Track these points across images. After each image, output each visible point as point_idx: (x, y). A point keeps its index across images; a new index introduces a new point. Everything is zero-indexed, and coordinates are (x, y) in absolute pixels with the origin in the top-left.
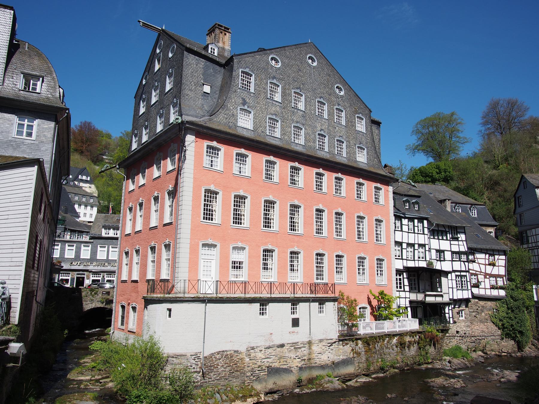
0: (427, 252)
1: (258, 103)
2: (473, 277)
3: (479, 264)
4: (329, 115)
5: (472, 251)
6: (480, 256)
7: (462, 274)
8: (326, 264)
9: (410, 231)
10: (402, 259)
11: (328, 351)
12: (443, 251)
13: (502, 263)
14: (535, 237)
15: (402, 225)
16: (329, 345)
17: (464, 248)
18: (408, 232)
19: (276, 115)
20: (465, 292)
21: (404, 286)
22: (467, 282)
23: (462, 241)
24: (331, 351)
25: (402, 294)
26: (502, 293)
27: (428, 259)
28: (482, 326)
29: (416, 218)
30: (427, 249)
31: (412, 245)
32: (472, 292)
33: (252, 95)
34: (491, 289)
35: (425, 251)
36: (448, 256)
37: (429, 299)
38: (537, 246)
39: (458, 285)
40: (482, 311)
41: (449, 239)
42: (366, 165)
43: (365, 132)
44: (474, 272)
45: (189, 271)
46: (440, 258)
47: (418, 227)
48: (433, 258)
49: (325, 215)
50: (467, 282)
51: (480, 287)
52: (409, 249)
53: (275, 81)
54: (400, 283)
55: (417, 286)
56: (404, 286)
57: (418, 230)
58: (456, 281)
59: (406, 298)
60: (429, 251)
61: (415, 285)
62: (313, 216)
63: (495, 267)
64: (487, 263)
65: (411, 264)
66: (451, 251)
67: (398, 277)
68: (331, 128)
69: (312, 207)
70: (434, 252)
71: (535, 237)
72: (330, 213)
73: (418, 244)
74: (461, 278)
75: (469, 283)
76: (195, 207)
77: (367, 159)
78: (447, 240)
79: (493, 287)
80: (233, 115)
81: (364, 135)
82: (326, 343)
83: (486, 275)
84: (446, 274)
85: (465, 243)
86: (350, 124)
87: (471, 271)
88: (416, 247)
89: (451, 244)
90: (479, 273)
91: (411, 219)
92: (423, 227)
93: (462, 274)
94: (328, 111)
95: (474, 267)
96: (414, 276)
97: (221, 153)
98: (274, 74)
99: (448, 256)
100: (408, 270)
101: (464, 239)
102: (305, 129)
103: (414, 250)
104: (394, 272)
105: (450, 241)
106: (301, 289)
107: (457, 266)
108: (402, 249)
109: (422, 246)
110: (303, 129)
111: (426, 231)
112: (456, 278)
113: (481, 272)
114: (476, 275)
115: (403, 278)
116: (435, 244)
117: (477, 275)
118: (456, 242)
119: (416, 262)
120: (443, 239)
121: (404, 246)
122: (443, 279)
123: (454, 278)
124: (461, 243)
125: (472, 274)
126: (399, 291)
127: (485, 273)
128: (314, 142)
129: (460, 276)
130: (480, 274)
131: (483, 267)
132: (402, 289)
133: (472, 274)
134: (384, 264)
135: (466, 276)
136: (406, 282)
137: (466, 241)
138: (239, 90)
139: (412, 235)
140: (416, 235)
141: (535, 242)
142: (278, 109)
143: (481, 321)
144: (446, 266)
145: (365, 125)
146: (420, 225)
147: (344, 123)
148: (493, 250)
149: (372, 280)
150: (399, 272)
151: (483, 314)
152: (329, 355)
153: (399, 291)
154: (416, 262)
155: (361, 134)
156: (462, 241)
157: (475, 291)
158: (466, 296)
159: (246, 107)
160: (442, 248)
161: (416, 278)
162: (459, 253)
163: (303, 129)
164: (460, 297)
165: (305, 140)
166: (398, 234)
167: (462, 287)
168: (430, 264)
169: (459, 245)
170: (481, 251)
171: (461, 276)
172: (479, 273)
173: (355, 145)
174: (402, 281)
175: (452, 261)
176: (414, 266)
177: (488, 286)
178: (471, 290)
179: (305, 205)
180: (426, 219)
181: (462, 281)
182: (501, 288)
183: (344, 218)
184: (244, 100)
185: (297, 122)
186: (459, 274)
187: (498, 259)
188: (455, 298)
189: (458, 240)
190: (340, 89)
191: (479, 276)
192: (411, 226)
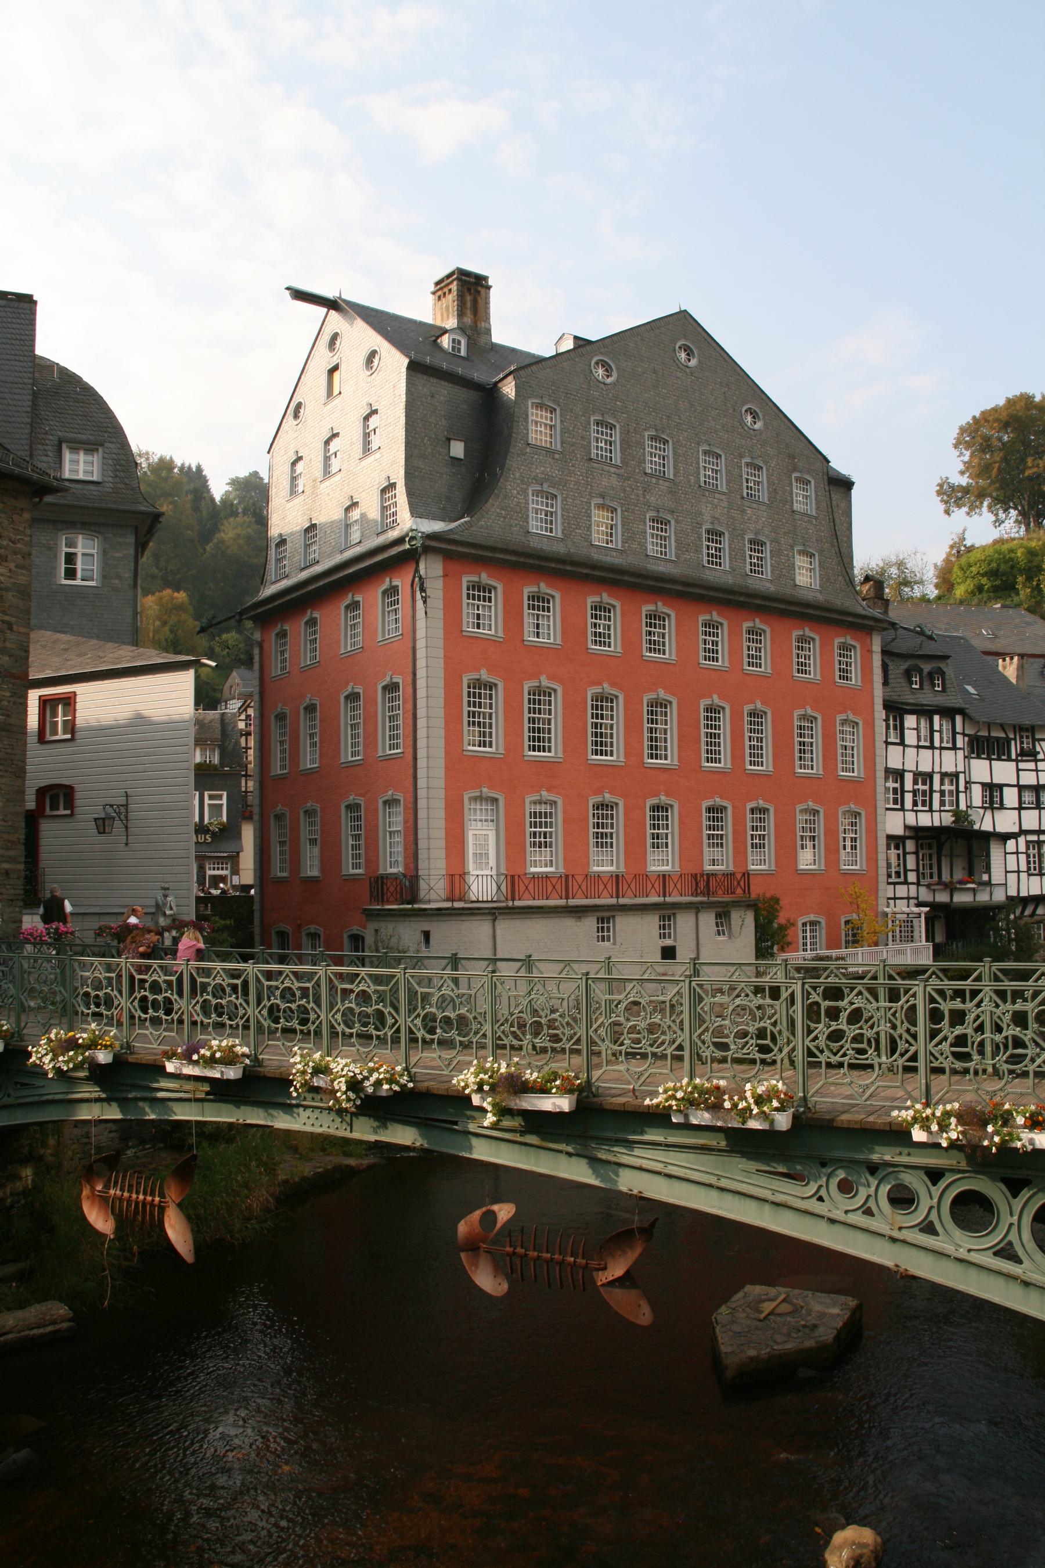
4: (728, 482)
10: (902, 809)
12: (1001, 787)
25: (902, 891)
27: (963, 806)
29: (936, 712)
31: (928, 777)
33: (557, 456)
37: (962, 898)
39: (1032, 865)
41: (1014, 757)
42: (818, 595)
43: (814, 513)
45: (448, 856)
46: (992, 802)
47: (940, 731)
48: (974, 805)
49: (725, 721)
55: (935, 870)
56: (906, 871)
58: (1028, 856)
59: (908, 898)
61: (931, 868)
62: (699, 722)
65: (925, 820)
68: (735, 514)
70: (977, 791)
72: (736, 716)
77: (821, 580)
78: (1009, 759)
81: (811, 523)
84: (1005, 837)
86: (780, 500)
88: (937, 779)
89: (1018, 770)
92: (954, 733)
94: (728, 472)
96: (930, 848)
99: (1011, 797)
100: (917, 833)
102: (677, 521)
104: (882, 842)
105: (1017, 761)
106: (679, 886)
112: (1028, 848)
116: (980, 770)
118: (1031, 765)
119: (936, 815)
120: (999, 759)
121: (909, 778)
122: (996, 853)
123: (1022, 848)
126: (895, 884)
128: (698, 551)
132: (902, 879)
138: (528, 450)
142: (614, 481)
144: (1006, 822)
145: (813, 496)
147: (764, 497)
153: (895, 884)
154: (936, 815)
155: (806, 519)
161: (934, 851)
163: (673, 522)
166: (895, 751)
169: (1037, 770)
173: (792, 547)
174: (901, 862)
175: (1020, 808)
176: (930, 824)
180: (961, 712)
186: (1034, 838)
188: (1024, 893)
189: (1036, 761)
190: (755, 416)
192: (924, 732)
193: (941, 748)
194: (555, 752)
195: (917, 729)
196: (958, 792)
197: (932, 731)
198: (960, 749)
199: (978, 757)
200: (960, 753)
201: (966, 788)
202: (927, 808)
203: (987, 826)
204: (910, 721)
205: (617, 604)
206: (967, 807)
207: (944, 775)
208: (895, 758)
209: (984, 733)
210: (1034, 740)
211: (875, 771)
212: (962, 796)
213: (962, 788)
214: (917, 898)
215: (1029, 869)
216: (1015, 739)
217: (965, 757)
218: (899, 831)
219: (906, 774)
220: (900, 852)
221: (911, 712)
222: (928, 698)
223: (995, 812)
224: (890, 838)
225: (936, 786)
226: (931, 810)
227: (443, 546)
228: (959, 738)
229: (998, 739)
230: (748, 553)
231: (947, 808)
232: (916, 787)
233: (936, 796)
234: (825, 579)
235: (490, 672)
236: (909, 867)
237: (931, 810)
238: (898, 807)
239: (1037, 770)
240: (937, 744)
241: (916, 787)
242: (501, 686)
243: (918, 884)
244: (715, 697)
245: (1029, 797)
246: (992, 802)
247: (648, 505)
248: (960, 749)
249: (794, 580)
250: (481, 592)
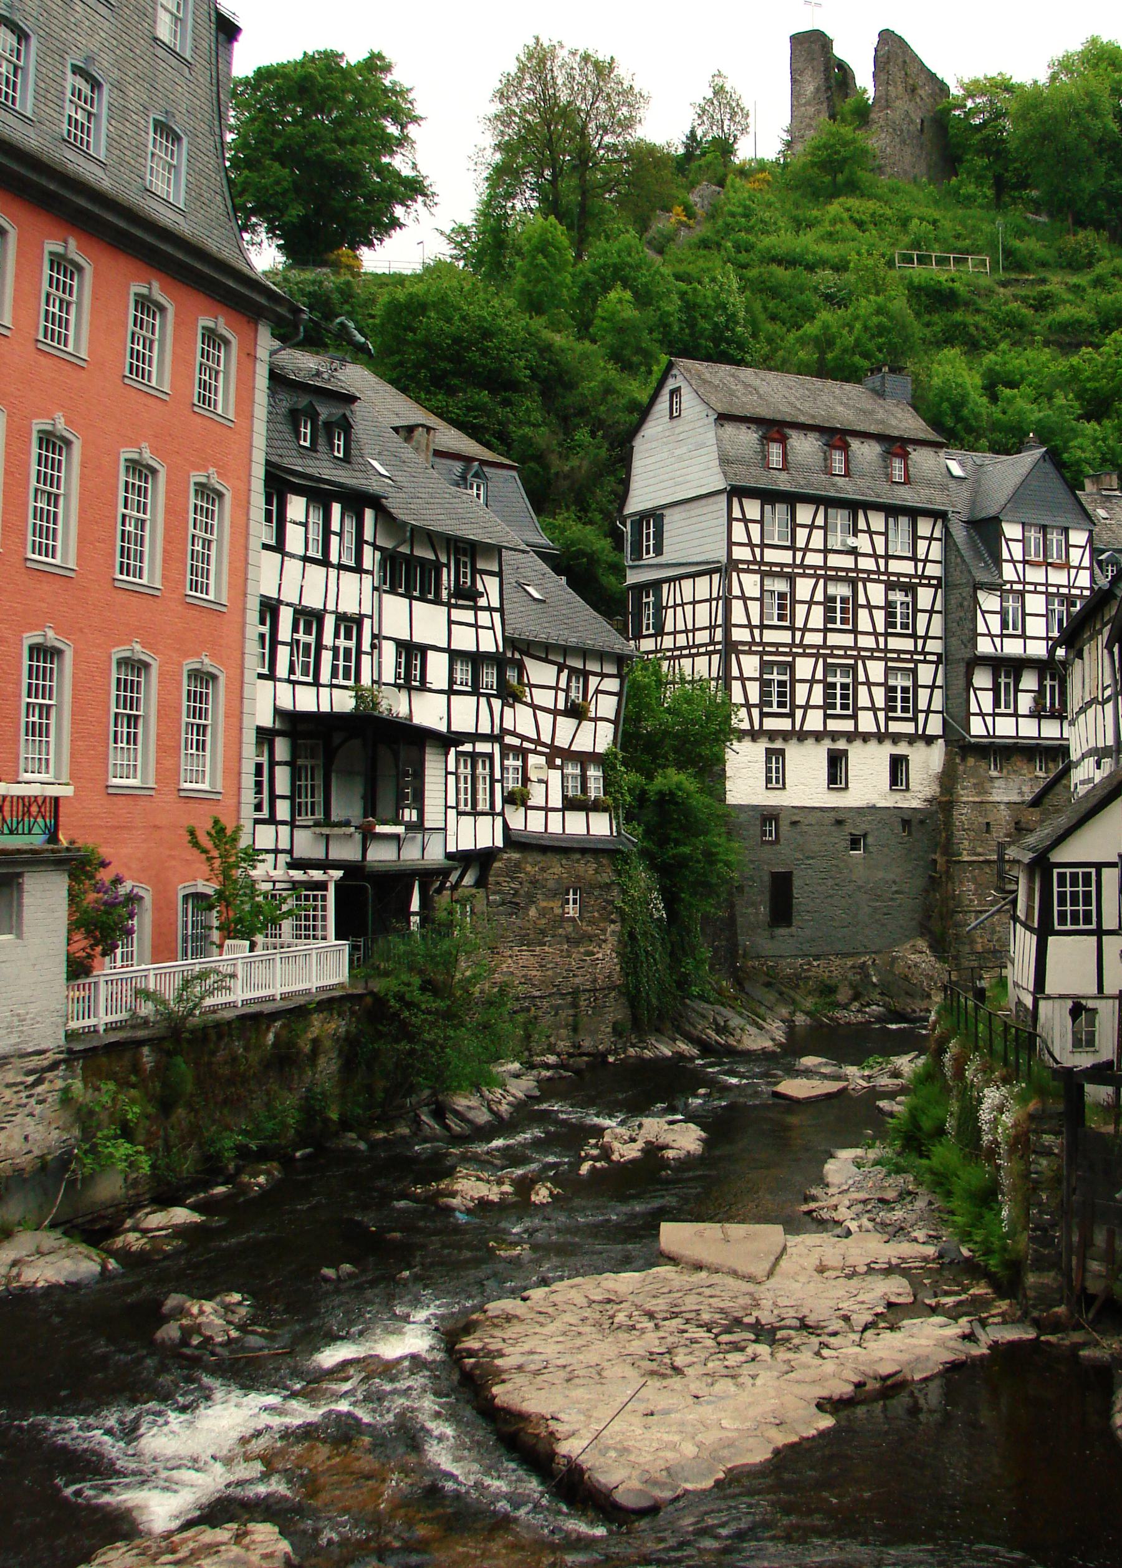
2: (510, 762)
3: (535, 707)
5: (517, 656)
6: (540, 672)
7: (483, 747)
11: (27, 1110)
12: (423, 649)
13: (607, 706)
14: (689, 609)
16: (31, 1079)
17: (488, 644)
20: (485, 822)
21: (273, 797)
23: (490, 609)
24: (38, 1109)
26: (601, 825)
27: (366, 680)
28: (526, 957)
32: (505, 825)
34: (563, 810)
38: (694, 646)
40: (531, 900)
44: (516, 742)
46: (408, 677)
47: (340, 534)
50: (493, 781)
51: (530, 803)
55: (319, 799)
56: (273, 797)
59: (276, 851)
63: (585, 723)
64: (561, 706)
65: (307, 701)
66: (448, 650)
70: (389, 649)
71: (689, 609)
73: (335, 612)
74: (474, 768)
75: (498, 786)
78: (437, 601)
79: (570, 805)
82: (18, 1074)
83: (556, 755)
85: (497, 616)
87: (509, 740)
88: (329, 622)
89: (450, 622)
90: (532, 746)
92: (360, 542)
93: (483, 747)
95: (521, 720)
99: (437, 668)
101: (495, 603)
104: (250, 737)
105: (450, 606)
109: (350, 623)
111: (370, 558)
113: (538, 742)
114: (522, 753)
115: (273, 764)
117: (522, 753)
118: (468, 616)
119: (324, 692)
120: (423, 599)
121: (286, 616)
123: (451, 767)
124: (484, 618)
127: (551, 746)
130: (535, 752)
131: (545, 719)
132: (265, 814)
133: (506, 750)
135: (491, 756)
136: (283, 777)
139: (316, 572)
140: (333, 573)
141: (686, 631)
143: (524, 940)
148: (585, 653)
149: (168, 774)
150: (265, 736)
151: (533, 912)
152: (31, 1127)
156: (490, 609)
157: (516, 819)
158: (484, 843)
162: (476, 659)
164: (466, 844)
169: (476, 626)
170: (544, 651)
171: (474, 756)
172: (532, 746)
175: (450, 692)
177: (556, 801)
178: (502, 814)
182: (595, 807)
186: (467, 747)
187: (597, 691)
189: (476, 609)
191: (533, 759)
192: (316, 533)
193: (341, 567)
195: (305, 525)
196: (359, 652)
197: (327, 532)
198: (367, 572)
199: (393, 591)
200: (367, 579)
201: (373, 646)
202: (310, 679)
204: (296, 507)
206: (373, 682)
209: (405, 549)
210: (475, 571)
211: (245, 595)
212: (366, 660)
213: (366, 647)
214: (290, 852)
216: (448, 566)
217: (375, 589)
218: (266, 720)
219: (282, 608)
220: (264, 760)
221: (299, 491)
222: (324, 469)
223: (413, 693)
224: (260, 730)
225: (328, 639)
226: (316, 683)
228: (367, 550)
229: (423, 562)
231: (340, 681)
232: (296, 636)
233: (327, 656)
236: (278, 792)
237: (316, 683)
238: (266, 671)
239: (476, 626)
240: (334, 559)
241: (296, 636)
243: (292, 824)
245: (463, 673)
246: (408, 677)
248: (367, 572)
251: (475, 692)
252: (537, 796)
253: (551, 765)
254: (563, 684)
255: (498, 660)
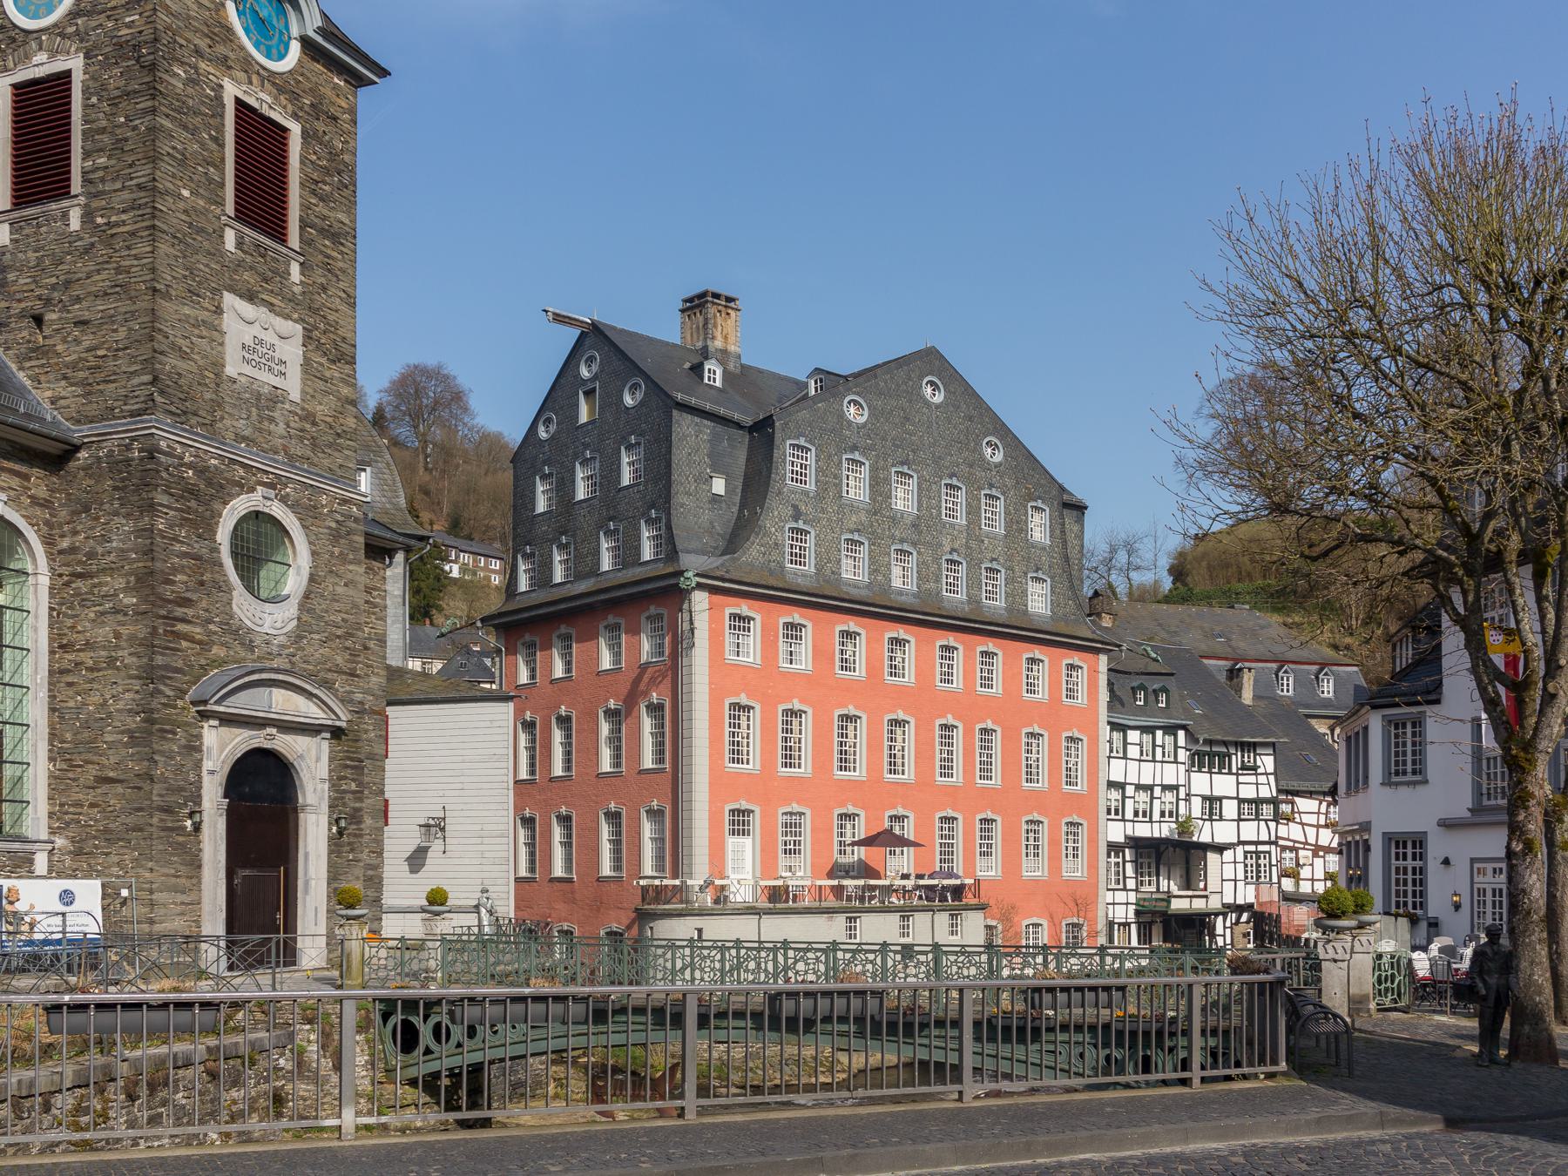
0: (1182, 803)
1: (823, 511)
2: (1287, 855)
6: (1303, 804)
7: (1261, 848)
8: (959, 841)
9: (1144, 757)
10: (1123, 820)
12: (1220, 799)
15: (1125, 744)
17: (1265, 793)
18: (1140, 761)
19: (858, 531)
22: (1271, 865)
30: (1182, 795)
31: (1150, 788)
35: (1178, 799)
36: (1230, 809)
39: (1249, 875)
41: (1234, 770)
44: (1291, 844)
46: (1211, 814)
47: (1163, 747)
49: (958, 736)
50: (1271, 865)
52: (1143, 797)
53: (857, 456)
54: (1118, 873)
57: (1164, 753)
58: (1246, 866)
60: (1186, 800)
64: (1322, 822)
66: (1237, 798)
67: (1113, 860)
69: (933, 721)
70: (1197, 803)
72: (968, 732)
74: (1258, 858)
75: (1274, 869)
76: (715, 740)
78: (1230, 773)
80: (776, 544)
87: (1281, 842)
89: (1238, 783)
91: (1149, 730)
92: (1176, 747)
93: (1261, 848)
95: (1294, 832)
96: (1149, 857)
97: (756, 627)
98: (854, 439)
99: (1230, 809)
101: (1270, 769)
103: (1152, 798)
105: (1237, 775)
107: (1249, 831)
108: (1124, 797)
110: (915, 553)
111: (1183, 755)
112: (1246, 858)
113: (1306, 843)
114: (1291, 849)
117: (1297, 850)
118: (1252, 779)
119: (1156, 826)
121: (1130, 790)
123: (1240, 858)
124: (1262, 779)
125: (1284, 848)
127: (1316, 845)
128: (938, 580)
129: (1255, 853)
131: (1311, 832)
134: (1083, 833)
135: (1269, 853)
137: (1275, 774)
139: (1147, 767)
144: (1223, 832)
146: (1169, 739)
159: (801, 525)
160: (1216, 793)
162: (1258, 802)
165: (919, 578)
167: (1258, 877)
168: (1185, 827)
169: (1257, 784)
171: (1257, 852)
175: (1240, 820)
177: (1320, 874)
179: (917, 720)
180: (1183, 727)
181: (1258, 866)
183: (997, 739)
184: (795, 507)
185: (902, 541)
186: (1252, 848)
189: (1256, 774)
191: (1301, 853)
192: (1148, 747)
194: (805, 769)
203: (1205, 838)
205: (863, 632)
207: (1165, 788)
208: (1117, 771)
215: (1246, 877)
227: (709, 582)
229: (1218, 754)
230: (984, 581)
231: (1167, 819)
234: (1055, 604)
235: (748, 696)
240: (1159, 757)
242: (758, 708)
244: (950, 716)
247: (893, 537)
249: (1026, 606)
250: (740, 621)
251: (1257, 819)
252: (1305, 873)
253: (1315, 855)
254: (1323, 809)
255: (1274, 802)
